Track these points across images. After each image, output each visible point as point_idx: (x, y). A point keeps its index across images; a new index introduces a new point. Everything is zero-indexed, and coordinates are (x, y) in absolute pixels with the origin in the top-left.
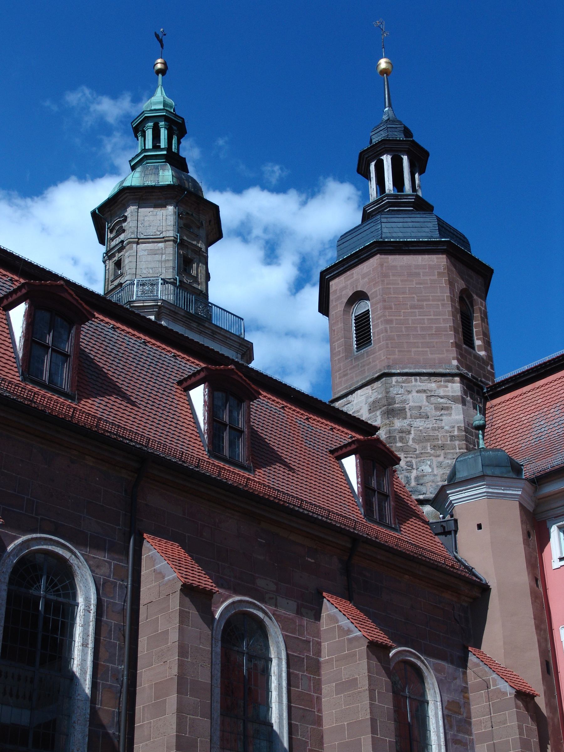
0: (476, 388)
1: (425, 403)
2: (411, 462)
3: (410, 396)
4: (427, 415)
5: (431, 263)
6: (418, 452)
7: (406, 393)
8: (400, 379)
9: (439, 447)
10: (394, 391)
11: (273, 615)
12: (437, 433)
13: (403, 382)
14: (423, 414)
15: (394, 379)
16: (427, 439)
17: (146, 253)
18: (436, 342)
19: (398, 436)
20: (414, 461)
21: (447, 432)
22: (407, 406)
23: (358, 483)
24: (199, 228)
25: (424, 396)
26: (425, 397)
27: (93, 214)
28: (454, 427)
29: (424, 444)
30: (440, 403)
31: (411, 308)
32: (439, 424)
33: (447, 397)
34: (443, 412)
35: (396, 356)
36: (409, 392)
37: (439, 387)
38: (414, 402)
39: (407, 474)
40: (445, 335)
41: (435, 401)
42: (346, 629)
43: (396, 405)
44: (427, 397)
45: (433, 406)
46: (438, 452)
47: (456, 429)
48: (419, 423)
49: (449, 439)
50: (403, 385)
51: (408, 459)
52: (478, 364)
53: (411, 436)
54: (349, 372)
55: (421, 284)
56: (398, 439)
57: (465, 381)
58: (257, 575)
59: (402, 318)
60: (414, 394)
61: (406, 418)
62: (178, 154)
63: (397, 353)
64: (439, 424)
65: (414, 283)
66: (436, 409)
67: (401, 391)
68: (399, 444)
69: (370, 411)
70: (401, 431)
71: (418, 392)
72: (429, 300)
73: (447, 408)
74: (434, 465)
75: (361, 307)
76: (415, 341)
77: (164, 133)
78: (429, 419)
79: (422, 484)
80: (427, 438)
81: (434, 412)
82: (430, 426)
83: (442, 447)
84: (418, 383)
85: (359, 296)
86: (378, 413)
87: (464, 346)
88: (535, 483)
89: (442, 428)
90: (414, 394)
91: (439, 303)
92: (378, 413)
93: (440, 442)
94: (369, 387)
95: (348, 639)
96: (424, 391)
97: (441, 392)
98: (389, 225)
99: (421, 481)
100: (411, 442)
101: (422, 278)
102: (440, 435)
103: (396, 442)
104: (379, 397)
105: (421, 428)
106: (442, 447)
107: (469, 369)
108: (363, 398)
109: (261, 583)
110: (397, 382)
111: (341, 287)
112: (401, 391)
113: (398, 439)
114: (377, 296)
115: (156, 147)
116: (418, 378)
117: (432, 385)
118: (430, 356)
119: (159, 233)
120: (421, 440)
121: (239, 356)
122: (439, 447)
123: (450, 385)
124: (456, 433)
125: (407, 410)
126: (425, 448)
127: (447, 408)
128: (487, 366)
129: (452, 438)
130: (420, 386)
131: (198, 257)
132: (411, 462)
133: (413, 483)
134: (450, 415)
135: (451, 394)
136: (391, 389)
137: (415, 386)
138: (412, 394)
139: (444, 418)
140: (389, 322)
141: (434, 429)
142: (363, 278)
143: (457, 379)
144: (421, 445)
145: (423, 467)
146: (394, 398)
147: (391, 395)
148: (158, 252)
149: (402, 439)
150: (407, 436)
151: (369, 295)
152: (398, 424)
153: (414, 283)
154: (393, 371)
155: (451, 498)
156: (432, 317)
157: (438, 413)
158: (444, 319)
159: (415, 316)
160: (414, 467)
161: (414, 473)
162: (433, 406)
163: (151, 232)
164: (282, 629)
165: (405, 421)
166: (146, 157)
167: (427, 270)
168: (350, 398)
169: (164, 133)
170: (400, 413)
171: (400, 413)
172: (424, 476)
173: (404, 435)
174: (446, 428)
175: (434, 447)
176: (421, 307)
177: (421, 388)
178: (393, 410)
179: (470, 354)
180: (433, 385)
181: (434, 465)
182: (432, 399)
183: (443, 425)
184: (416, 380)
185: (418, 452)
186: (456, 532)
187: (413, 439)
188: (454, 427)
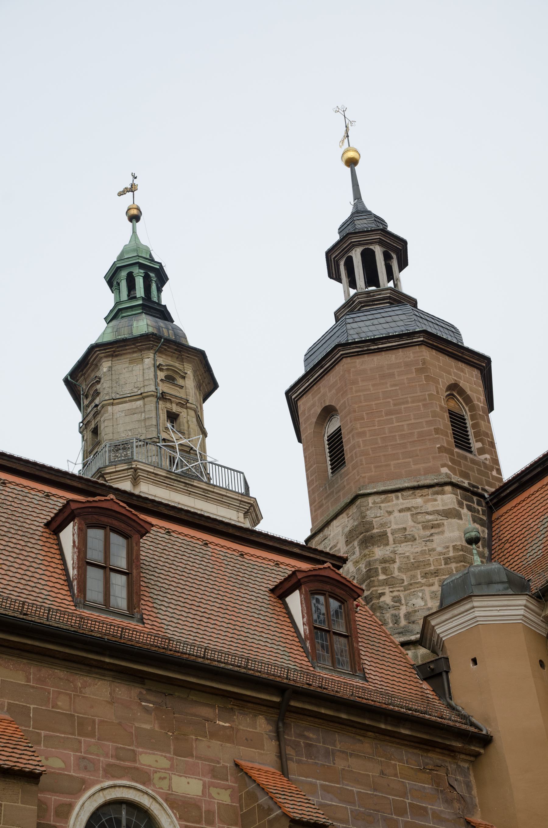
0: (475, 498)
1: (411, 523)
2: (398, 597)
3: (392, 517)
4: (413, 536)
5: (407, 360)
6: (406, 583)
7: (387, 514)
8: (377, 498)
9: (432, 574)
10: (370, 514)
11: (166, 800)
12: (427, 557)
13: (382, 502)
14: (409, 537)
15: (371, 500)
16: (416, 566)
17: (123, 414)
18: (420, 450)
19: (379, 567)
20: (402, 595)
21: (440, 554)
22: (389, 531)
23: (304, 624)
24: (184, 378)
25: (408, 514)
26: (409, 517)
27: (66, 381)
28: (448, 547)
29: (412, 573)
30: (429, 521)
31: (387, 415)
32: (430, 545)
33: (438, 512)
34: (433, 531)
35: (373, 473)
36: (390, 513)
37: (426, 502)
38: (396, 524)
39: (394, 612)
40: (430, 440)
41: (424, 520)
42: (266, 807)
43: (375, 531)
44: (412, 515)
45: (420, 526)
46: (431, 580)
47: (451, 549)
48: (405, 549)
49: (443, 562)
50: (382, 505)
51: (395, 594)
52: (478, 470)
53: (396, 566)
54: (324, 502)
55: (395, 385)
56: (380, 571)
57: (459, 491)
58: (140, 750)
59: (376, 428)
60: (396, 514)
61: (387, 544)
62: (159, 304)
63: (373, 469)
64: (430, 545)
65: (388, 385)
66: (424, 528)
67: (379, 513)
68: (382, 577)
69: (347, 543)
70: (384, 561)
71: (400, 511)
72: (407, 402)
73: (439, 526)
74: (428, 597)
76: (394, 452)
77: (139, 282)
78: (417, 542)
79: (413, 622)
80: (416, 565)
81: (422, 533)
82: (419, 550)
83: (436, 573)
84: (401, 500)
85: (328, 412)
86: (356, 543)
87: (456, 450)
88: (541, 598)
89: (434, 550)
90: (396, 514)
91: (420, 404)
92: (356, 543)
93: (432, 568)
94: (344, 515)
95: (270, 821)
96: (409, 509)
97: (430, 507)
98: (354, 325)
99: (413, 619)
100: (396, 573)
101: (397, 378)
102: (431, 559)
103: (378, 575)
104: (356, 524)
105: (407, 554)
108: (340, 529)
109: (147, 759)
110: (374, 503)
112: (379, 513)
113: (380, 571)
114: (345, 408)
115: (132, 297)
116: (399, 494)
117: (417, 501)
118: (414, 467)
119: (136, 390)
120: (407, 568)
121: (241, 515)
122: (432, 574)
123: (439, 497)
124: (451, 554)
125: (389, 535)
126: (414, 577)
127: (439, 526)
128: (492, 470)
129: (447, 561)
130: (403, 504)
131: (185, 410)
132: (398, 597)
133: (403, 622)
134: (442, 532)
135: (441, 508)
136: (368, 513)
137: (397, 505)
138: (393, 515)
139: (435, 538)
141: (423, 553)
142: (330, 391)
143: (448, 488)
144: (409, 573)
145: (414, 601)
146: (371, 523)
147: (368, 519)
148: (137, 411)
149: (385, 571)
150: (392, 566)
151: (337, 408)
152: (379, 552)
153: (388, 385)
154: (369, 491)
155: (438, 631)
156: (413, 421)
157: (428, 533)
158: (427, 422)
159: (393, 423)
160: (403, 602)
161: (403, 610)
162: (420, 526)
163: (127, 390)
164: (180, 818)
165: (388, 548)
166: (120, 310)
167: (403, 369)
168: (326, 531)
169: (139, 282)
170: (382, 539)
171: (382, 539)
172: (415, 611)
173: (387, 565)
174: (439, 549)
175: (425, 575)
177: (404, 506)
178: (372, 537)
179: (465, 458)
180: (419, 501)
181: (428, 597)
182: (419, 517)
183: (434, 546)
184: (397, 498)
185: (406, 583)
186: (447, 672)
187: (400, 569)
188: (448, 547)
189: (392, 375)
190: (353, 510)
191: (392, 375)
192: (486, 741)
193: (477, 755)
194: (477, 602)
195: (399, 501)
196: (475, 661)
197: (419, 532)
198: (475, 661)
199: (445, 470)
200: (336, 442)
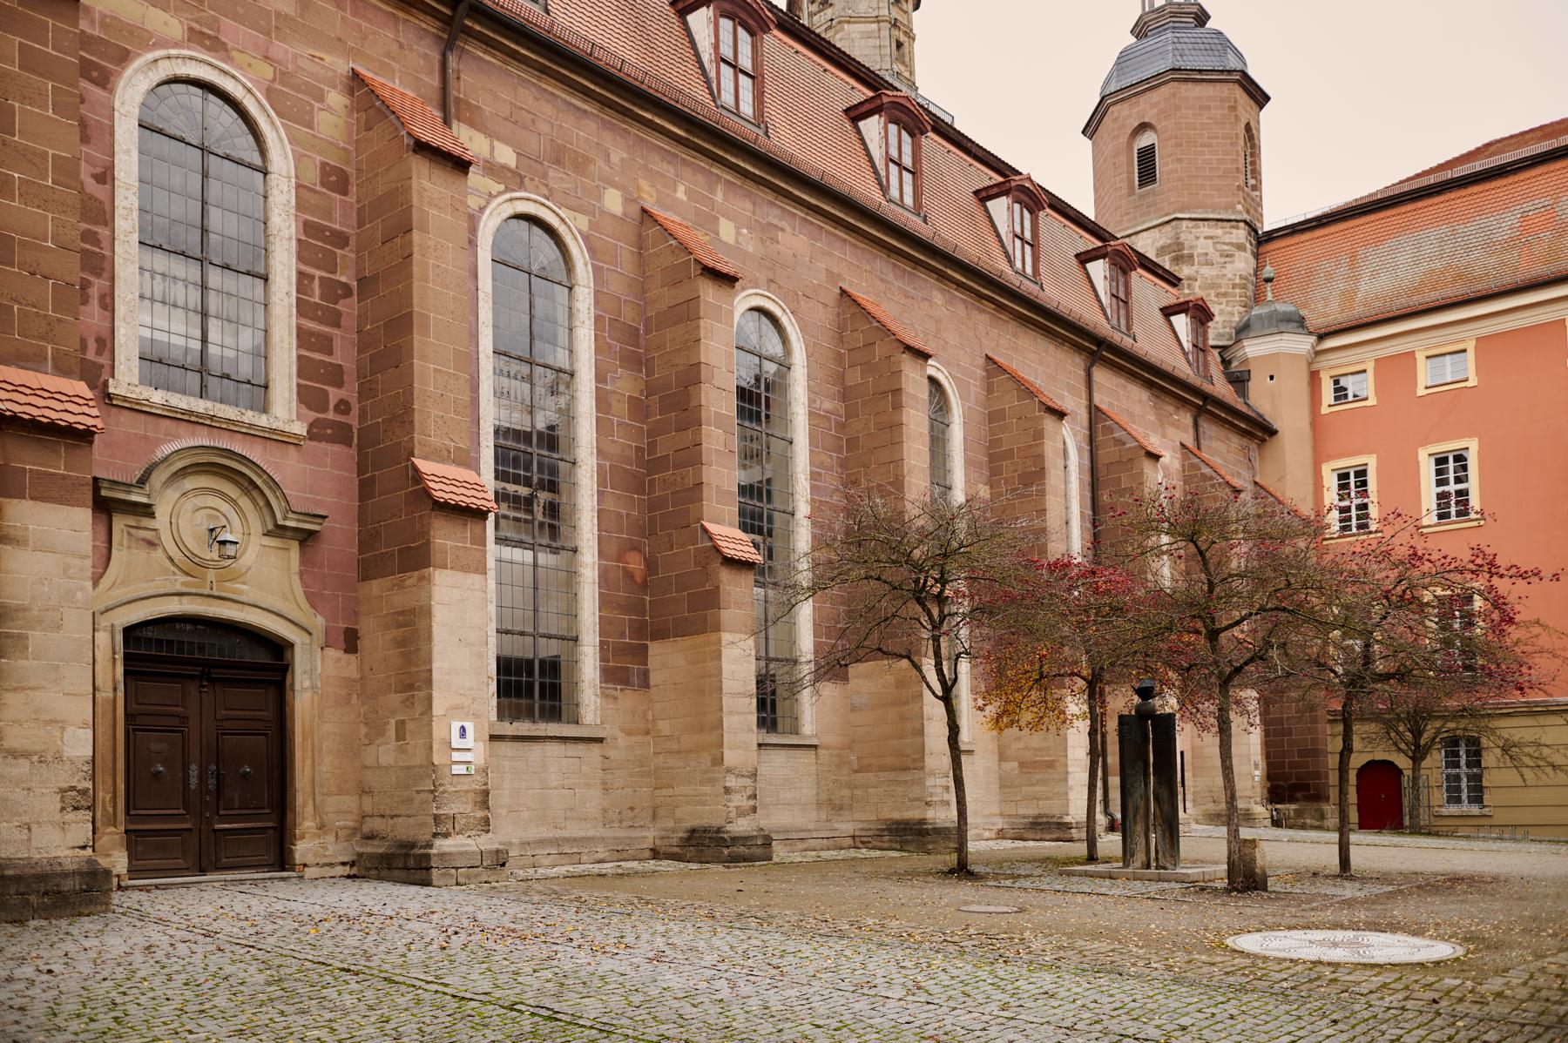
10: (1183, 237)
15: (1184, 223)
32: (1224, 271)
64: (1224, 271)
70: (1189, 278)
75: (1146, 140)
83: (1225, 295)
106: (1225, 295)
107: (1248, 212)
111: (1126, 115)
124: (1237, 281)
129: (1234, 287)
138: (1200, 240)
140: (1179, 160)
175: (1217, 295)
176: (1210, 145)
180: (1219, 232)
189: (1208, 108)
190: (1168, 228)
191: (1208, 108)
192: (1273, 432)
193: (1263, 441)
194: (1285, 336)
195: (1205, 230)
196: (1272, 378)
197: (1216, 258)
198: (1272, 378)
199: (1239, 207)
200: (1147, 159)
